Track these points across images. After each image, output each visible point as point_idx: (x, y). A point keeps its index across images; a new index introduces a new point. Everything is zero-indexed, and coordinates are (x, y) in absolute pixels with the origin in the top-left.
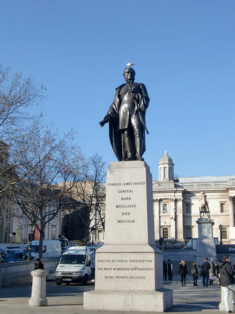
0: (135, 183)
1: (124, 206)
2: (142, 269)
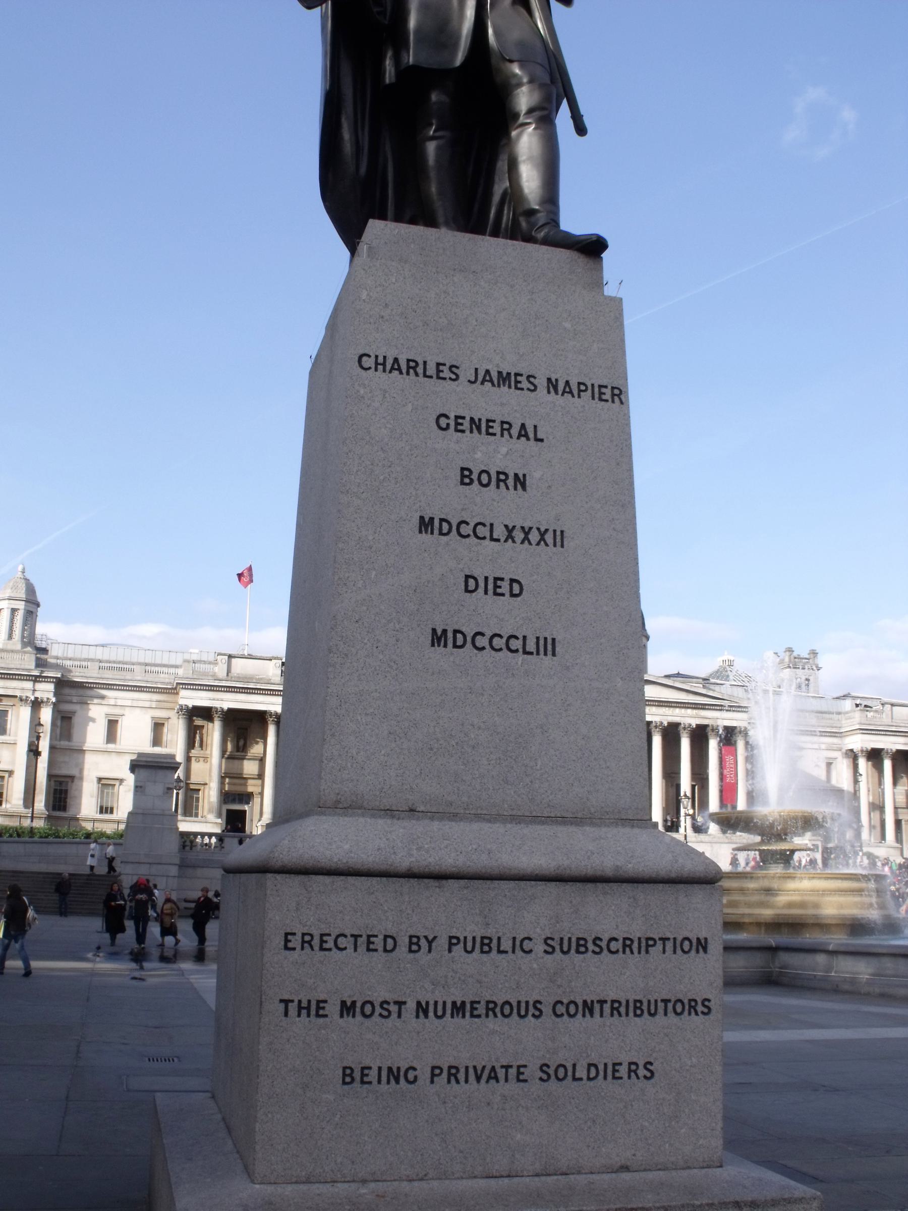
0: (552, 385)
2: (638, 1008)
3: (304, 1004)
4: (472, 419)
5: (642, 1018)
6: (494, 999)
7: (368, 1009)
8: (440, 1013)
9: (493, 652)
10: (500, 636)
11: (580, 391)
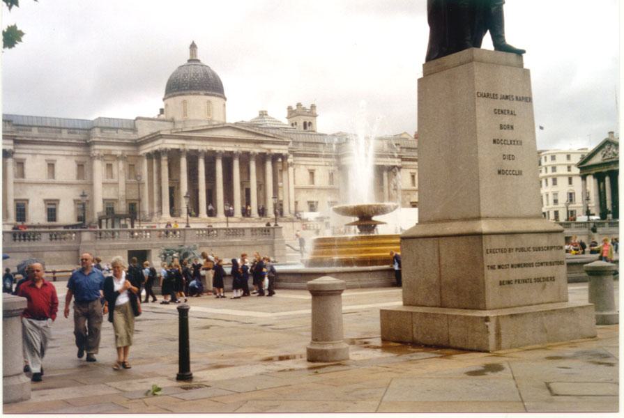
0: (517, 98)
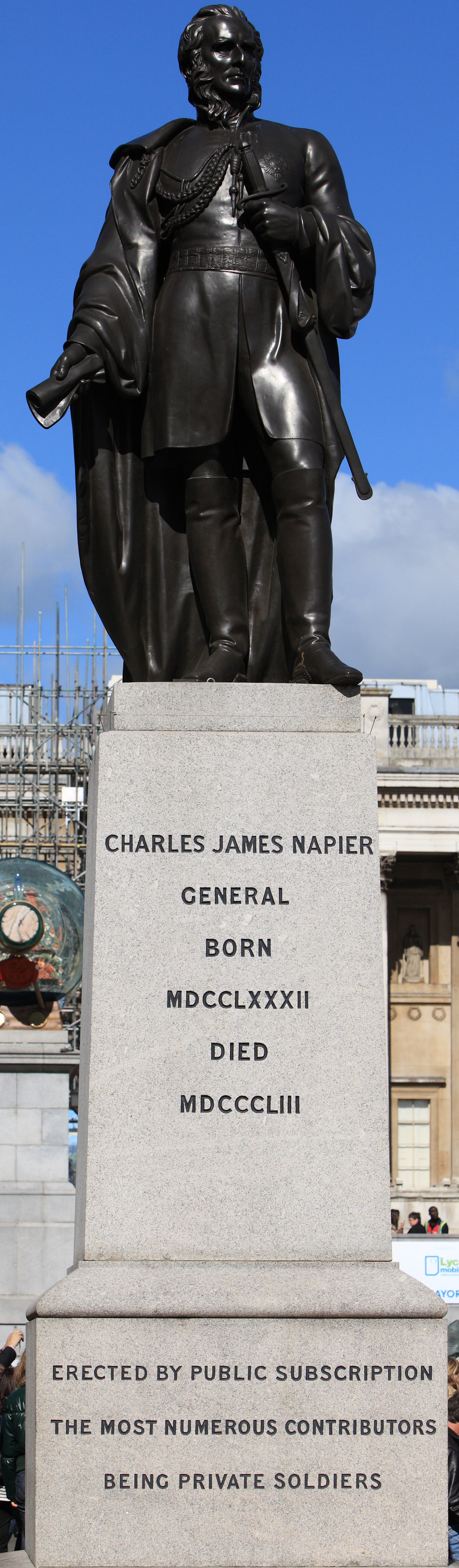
0: (298, 843)
1: (227, 1000)
2: (365, 1427)
3: (71, 1423)
4: (217, 889)
5: (369, 1436)
6: (233, 1419)
7: (124, 1427)
8: (186, 1430)
9: (239, 1114)
10: (246, 1098)
11: (327, 845)
